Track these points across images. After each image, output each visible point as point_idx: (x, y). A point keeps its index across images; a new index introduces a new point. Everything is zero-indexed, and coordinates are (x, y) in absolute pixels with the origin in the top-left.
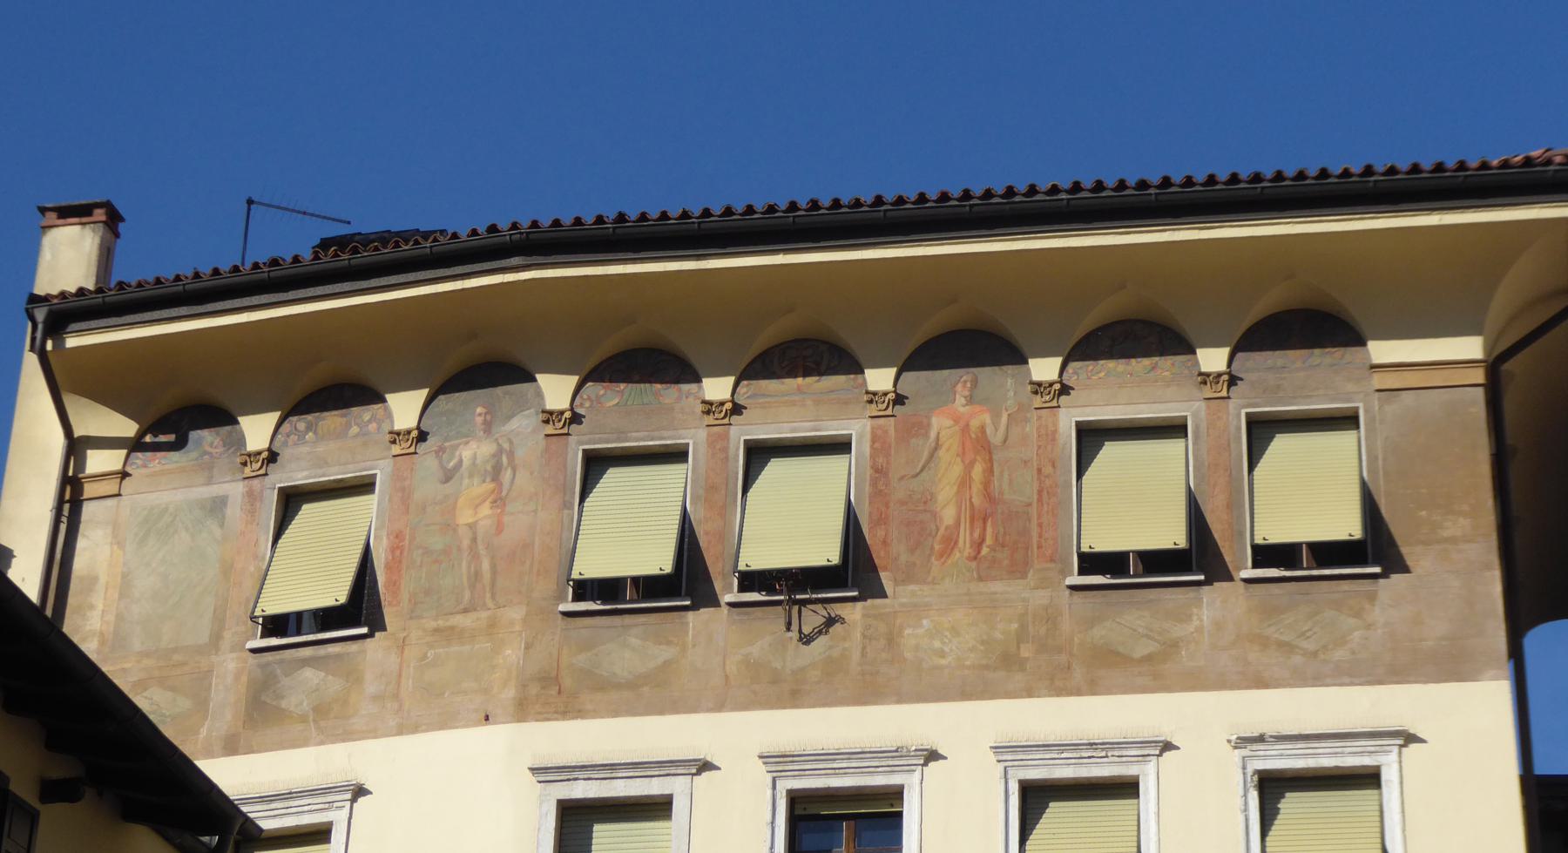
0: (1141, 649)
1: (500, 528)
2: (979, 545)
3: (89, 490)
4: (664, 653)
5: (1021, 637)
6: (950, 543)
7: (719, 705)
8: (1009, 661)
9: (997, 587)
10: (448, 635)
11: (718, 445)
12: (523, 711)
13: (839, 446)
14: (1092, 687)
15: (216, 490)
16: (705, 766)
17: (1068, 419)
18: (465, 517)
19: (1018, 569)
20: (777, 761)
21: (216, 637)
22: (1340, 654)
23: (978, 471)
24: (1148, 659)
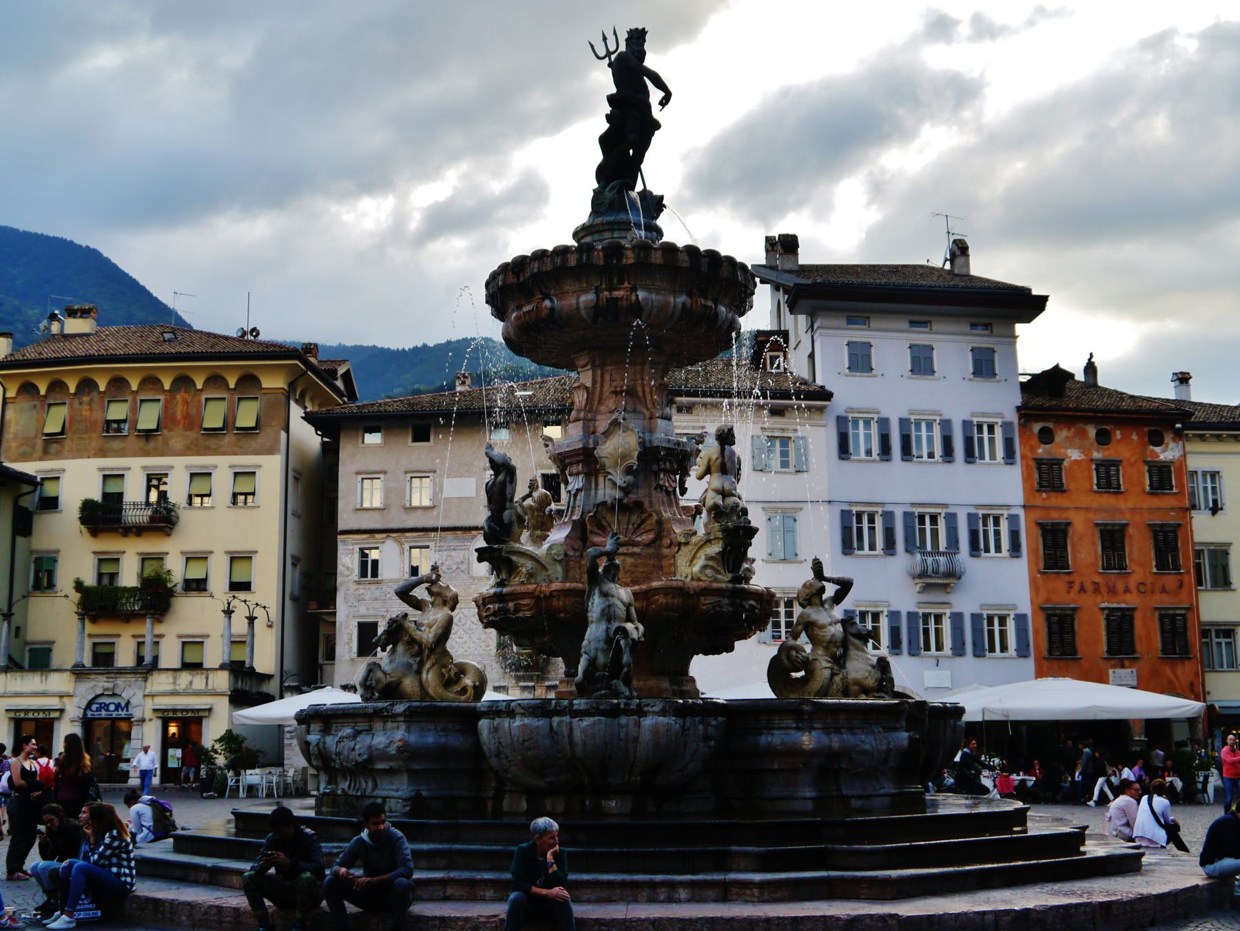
0: (214, 447)
1: (91, 416)
2: (184, 424)
3: (8, 401)
4: (123, 445)
5: (192, 443)
6: (179, 423)
7: (134, 456)
8: (189, 448)
9: (188, 433)
10: (81, 439)
11: (134, 401)
12: (96, 456)
13: (159, 400)
14: (204, 454)
15: (36, 403)
16: (130, 468)
17: (203, 397)
18: (84, 413)
19: (192, 429)
20: (144, 468)
21: (36, 435)
22: (251, 449)
23: (185, 408)
24: (215, 449)
